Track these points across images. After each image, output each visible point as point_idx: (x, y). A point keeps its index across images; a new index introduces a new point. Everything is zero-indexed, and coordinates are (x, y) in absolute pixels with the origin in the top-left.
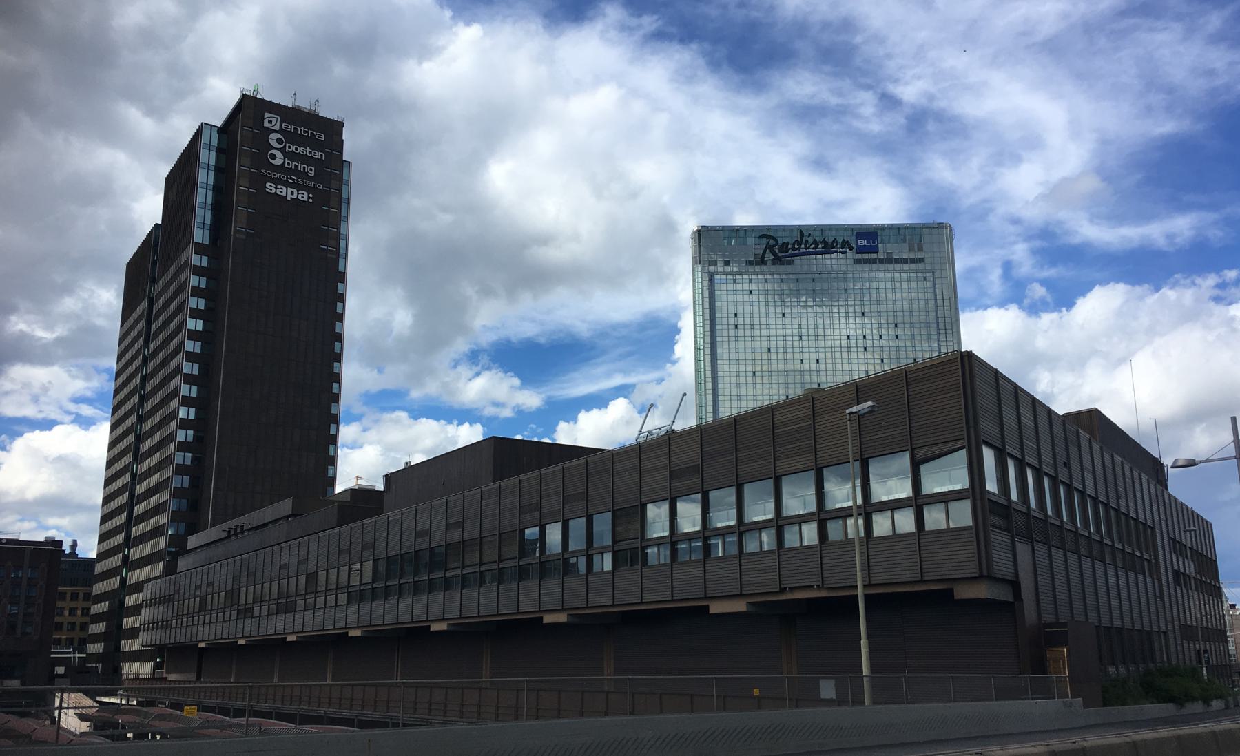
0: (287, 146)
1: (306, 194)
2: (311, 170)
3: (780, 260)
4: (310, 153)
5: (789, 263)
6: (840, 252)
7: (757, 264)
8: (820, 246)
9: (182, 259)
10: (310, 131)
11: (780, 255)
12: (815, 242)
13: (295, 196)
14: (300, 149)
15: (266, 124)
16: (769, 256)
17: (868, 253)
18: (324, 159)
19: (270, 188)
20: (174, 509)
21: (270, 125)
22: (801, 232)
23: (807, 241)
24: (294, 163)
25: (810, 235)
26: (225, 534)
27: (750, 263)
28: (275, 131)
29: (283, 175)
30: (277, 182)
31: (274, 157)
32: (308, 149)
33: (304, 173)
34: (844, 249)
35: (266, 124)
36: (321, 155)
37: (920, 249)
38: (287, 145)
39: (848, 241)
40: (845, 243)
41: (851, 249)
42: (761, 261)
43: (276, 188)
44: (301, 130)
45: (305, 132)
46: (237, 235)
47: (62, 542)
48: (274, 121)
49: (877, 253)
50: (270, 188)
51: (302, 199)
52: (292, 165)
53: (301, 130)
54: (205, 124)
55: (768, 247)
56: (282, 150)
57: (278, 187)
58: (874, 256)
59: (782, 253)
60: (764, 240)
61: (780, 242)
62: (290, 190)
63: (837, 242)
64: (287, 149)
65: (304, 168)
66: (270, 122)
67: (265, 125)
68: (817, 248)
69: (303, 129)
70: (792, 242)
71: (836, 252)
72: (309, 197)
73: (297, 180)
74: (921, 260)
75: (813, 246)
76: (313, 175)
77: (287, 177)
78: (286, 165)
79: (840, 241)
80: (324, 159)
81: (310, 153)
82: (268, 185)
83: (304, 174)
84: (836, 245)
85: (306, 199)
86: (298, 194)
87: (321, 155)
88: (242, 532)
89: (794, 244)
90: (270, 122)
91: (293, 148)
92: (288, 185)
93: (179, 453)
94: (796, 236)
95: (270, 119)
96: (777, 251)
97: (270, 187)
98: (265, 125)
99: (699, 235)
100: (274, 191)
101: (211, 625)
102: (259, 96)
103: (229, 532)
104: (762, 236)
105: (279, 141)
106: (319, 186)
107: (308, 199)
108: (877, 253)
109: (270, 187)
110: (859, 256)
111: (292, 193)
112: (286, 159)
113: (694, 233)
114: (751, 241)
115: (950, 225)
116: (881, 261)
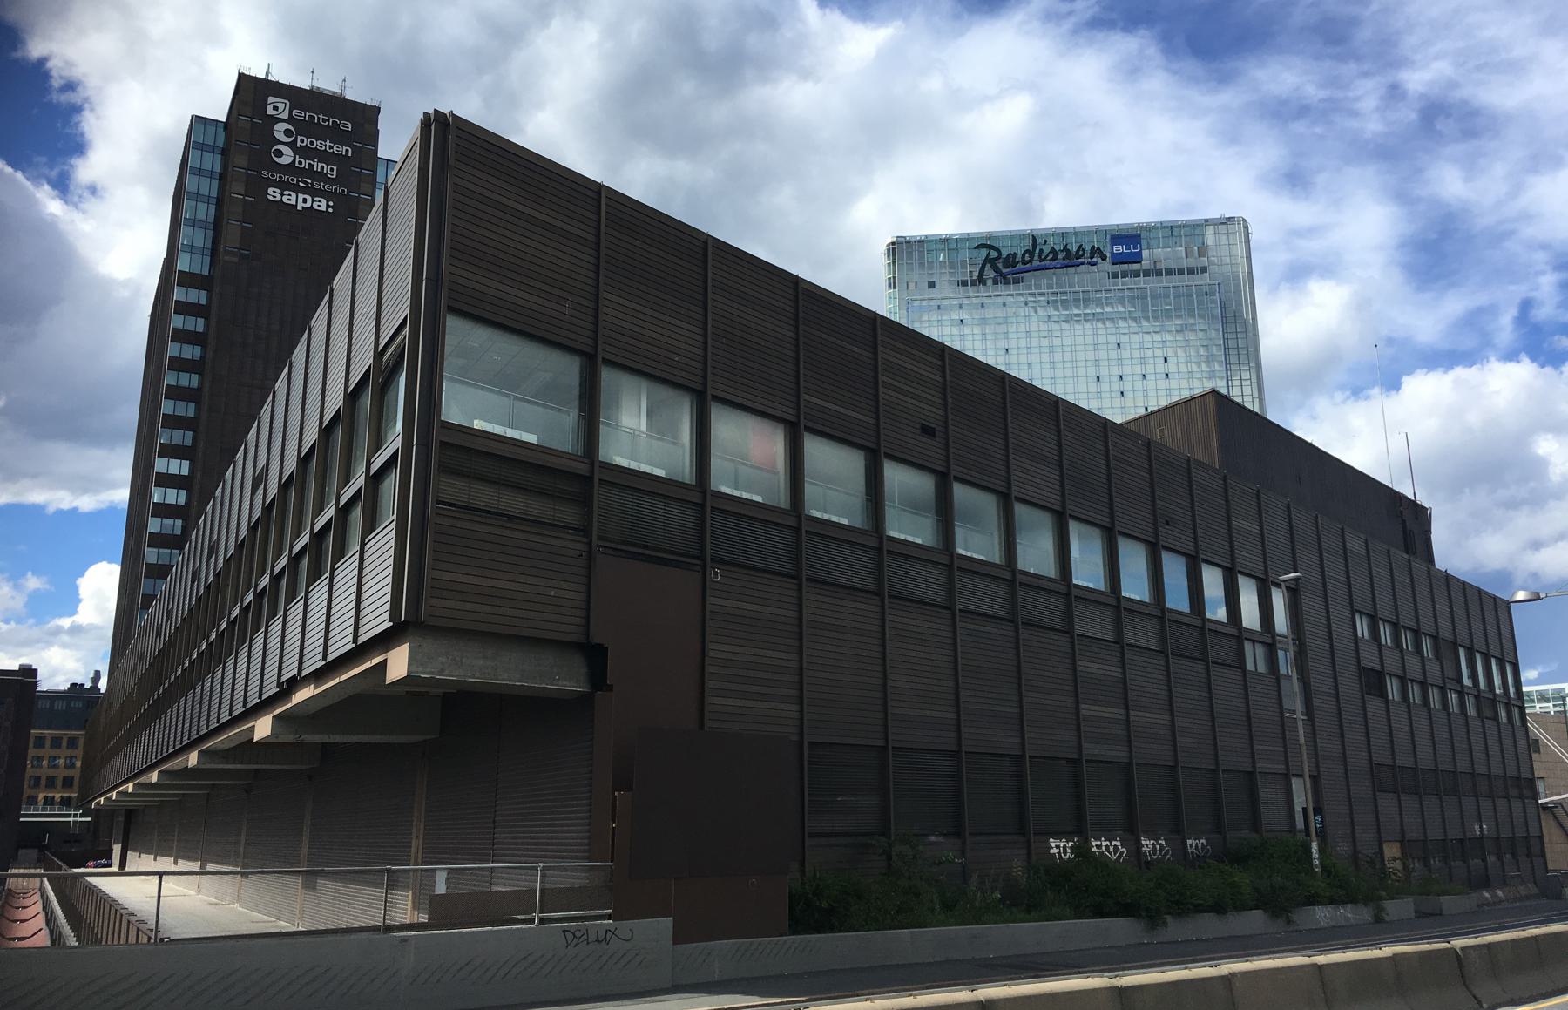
0: (299, 141)
1: (324, 201)
2: (332, 170)
3: (1005, 278)
4: (331, 147)
5: (1017, 281)
6: (1089, 263)
7: (973, 283)
8: (1060, 257)
10: (331, 120)
11: (1004, 271)
12: (1053, 250)
13: (308, 205)
14: (317, 144)
15: (270, 111)
16: (990, 273)
17: (1130, 263)
18: (350, 155)
19: (274, 194)
21: (277, 113)
22: (1033, 236)
23: (1041, 251)
24: (307, 162)
25: (1045, 241)
27: (964, 283)
29: (292, 178)
30: (283, 186)
31: (279, 154)
32: (328, 143)
34: (1095, 259)
35: (270, 111)
36: (347, 150)
37: (1202, 251)
38: (299, 138)
39: (1098, 248)
40: (1095, 251)
41: (1104, 258)
42: (981, 280)
43: (282, 195)
44: (319, 118)
45: (324, 120)
48: (281, 107)
49: (1140, 262)
51: (319, 208)
52: (306, 164)
53: (319, 118)
55: (987, 260)
56: (292, 145)
57: (285, 193)
58: (1136, 266)
59: (1005, 267)
60: (984, 252)
61: (1004, 254)
62: (301, 197)
63: (1083, 250)
64: (299, 144)
65: (322, 167)
66: (276, 108)
67: (268, 113)
68: (1056, 259)
69: (321, 116)
70: (1020, 252)
71: (1083, 263)
72: (327, 204)
73: (312, 184)
74: (1204, 270)
75: (1051, 256)
76: (334, 176)
77: (298, 181)
78: (297, 165)
79: (1088, 248)
80: (350, 155)
81: (331, 147)
82: (270, 191)
83: (322, 175)
84: (1083, 255)
86: (313, 201)
87: (347, 150)
89: (1023, 255)
90: (276, 108)
91: (307, 142)
92: (298, 190)
94: (1029, 245)
95: (275, 104)
96: (1000, 266)
97: (273, 194)
98: (268, 113)
99: (894, 249)
100: (278, 198)
104: (979, 247)
105: (287, 133)
106: (343, 191)
107: (327, 209)
108: (1140, 262)
109: (273, 194)
110: (1117, 268)
111: (305, 201)
112: (297, 157)
113: (888, 245)
114: (965, 255)
115: (1244, 220)
116: (1147, 273)
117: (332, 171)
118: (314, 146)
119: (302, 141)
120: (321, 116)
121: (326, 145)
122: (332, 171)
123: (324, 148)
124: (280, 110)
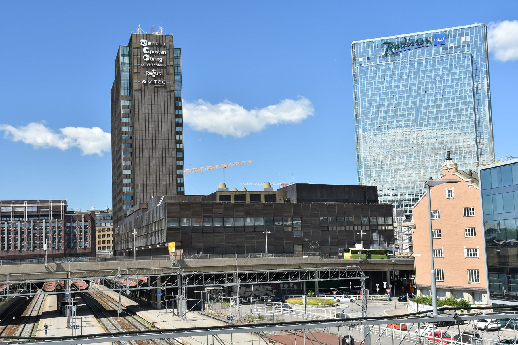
2: (161, 60)
4: (160, 52)
21: (143, 44)
32: (159, 51)
33: (158, 62)
35: (142, 44)
48: (144, 42)
56: (149, 54)
64: (151, 53)
65: (158, 59)
66: (143, 43)
68: (414, 45)
78: (151, 60)
81: (160, 52)
90: (143, 43)
91: (153, 52)
95: (143, 42)
105: (147, 50)
117: (160, 60)
119: (151, 52)
122: (160, 60)
124: (144, 43)
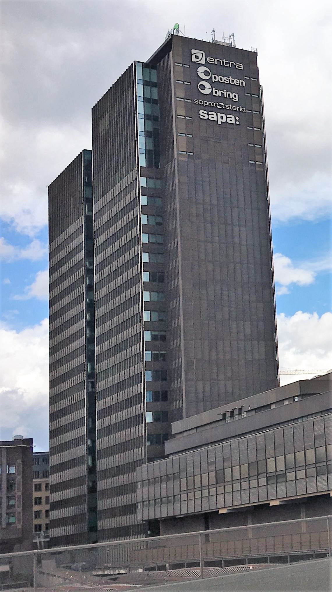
1: (233, 117)
9: (127, 180)
10: (230, 63)
13: (224, 120)
15: (194, 59)
18: (244, 85)
19: (203, 114)
20: (148, 401)
21: (197, 60)
26: (221, 417)
28: (202, 65)
30: (209, 109)
31: (203, 87)
32: (230, 78)
35: (194, 59)
36: (242, 83)
43: (208, 115)
44: (223, 62)
46: (180, 158)
47: (32, 439)
48: (200, 56)
50: (203, 114)
53: (223, 62)
54: (137, 62)
56: (209, 81)
62: (219, 115)
64: (214, 80)
65: (229, 94)
66: (197, 57)
69: (224, 61)
72: (235, 119)
73: (225, 106)
76: (237, 100)
77: (216, 104)
80: (244, 85)
81: (233, 81)
82: (201, 112)
85: (233, 122)
86: (227, 118)
87: (242, 83)
88: (240, 414)
90: (197, 57)
91: (218, 78)
92: (217, 111)
93: (147, 352)
95: (197, 55)
100: (206, 117)
101: (251, 491)
102: (180, 34)
103: (224, 415)
105: (206, 73)
107: (235, 122)
118: (223, 81)
120: (224, 61)
121: (229, 80)
123: (228, 82)
124: (200, 58)
